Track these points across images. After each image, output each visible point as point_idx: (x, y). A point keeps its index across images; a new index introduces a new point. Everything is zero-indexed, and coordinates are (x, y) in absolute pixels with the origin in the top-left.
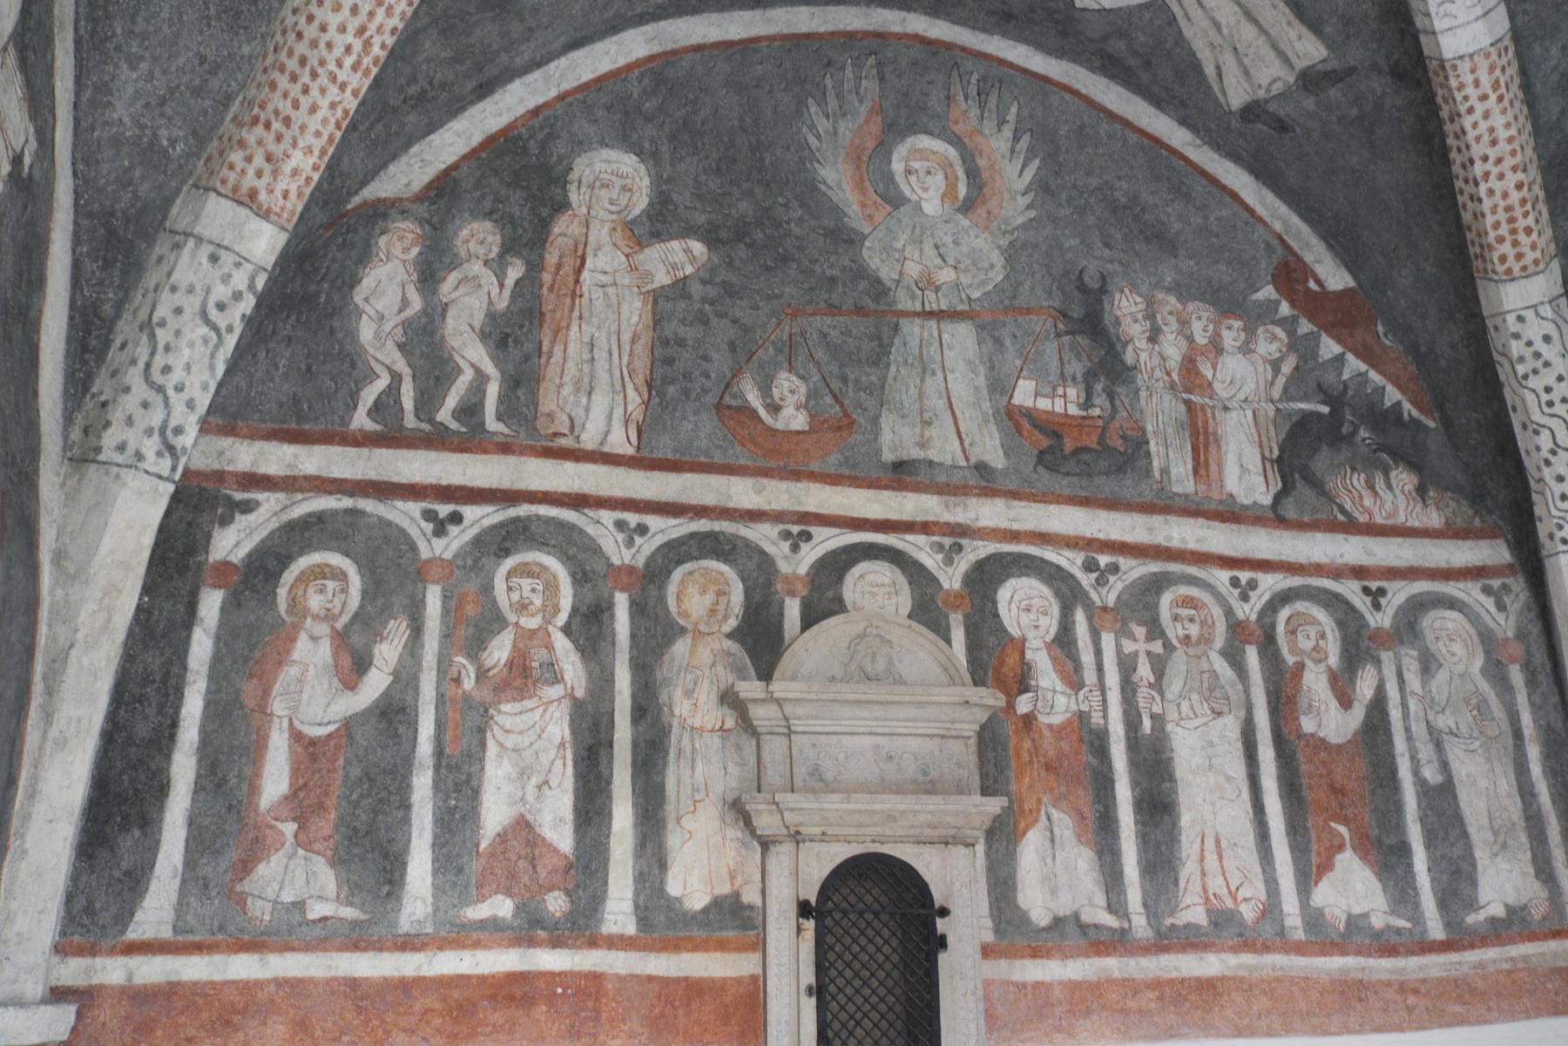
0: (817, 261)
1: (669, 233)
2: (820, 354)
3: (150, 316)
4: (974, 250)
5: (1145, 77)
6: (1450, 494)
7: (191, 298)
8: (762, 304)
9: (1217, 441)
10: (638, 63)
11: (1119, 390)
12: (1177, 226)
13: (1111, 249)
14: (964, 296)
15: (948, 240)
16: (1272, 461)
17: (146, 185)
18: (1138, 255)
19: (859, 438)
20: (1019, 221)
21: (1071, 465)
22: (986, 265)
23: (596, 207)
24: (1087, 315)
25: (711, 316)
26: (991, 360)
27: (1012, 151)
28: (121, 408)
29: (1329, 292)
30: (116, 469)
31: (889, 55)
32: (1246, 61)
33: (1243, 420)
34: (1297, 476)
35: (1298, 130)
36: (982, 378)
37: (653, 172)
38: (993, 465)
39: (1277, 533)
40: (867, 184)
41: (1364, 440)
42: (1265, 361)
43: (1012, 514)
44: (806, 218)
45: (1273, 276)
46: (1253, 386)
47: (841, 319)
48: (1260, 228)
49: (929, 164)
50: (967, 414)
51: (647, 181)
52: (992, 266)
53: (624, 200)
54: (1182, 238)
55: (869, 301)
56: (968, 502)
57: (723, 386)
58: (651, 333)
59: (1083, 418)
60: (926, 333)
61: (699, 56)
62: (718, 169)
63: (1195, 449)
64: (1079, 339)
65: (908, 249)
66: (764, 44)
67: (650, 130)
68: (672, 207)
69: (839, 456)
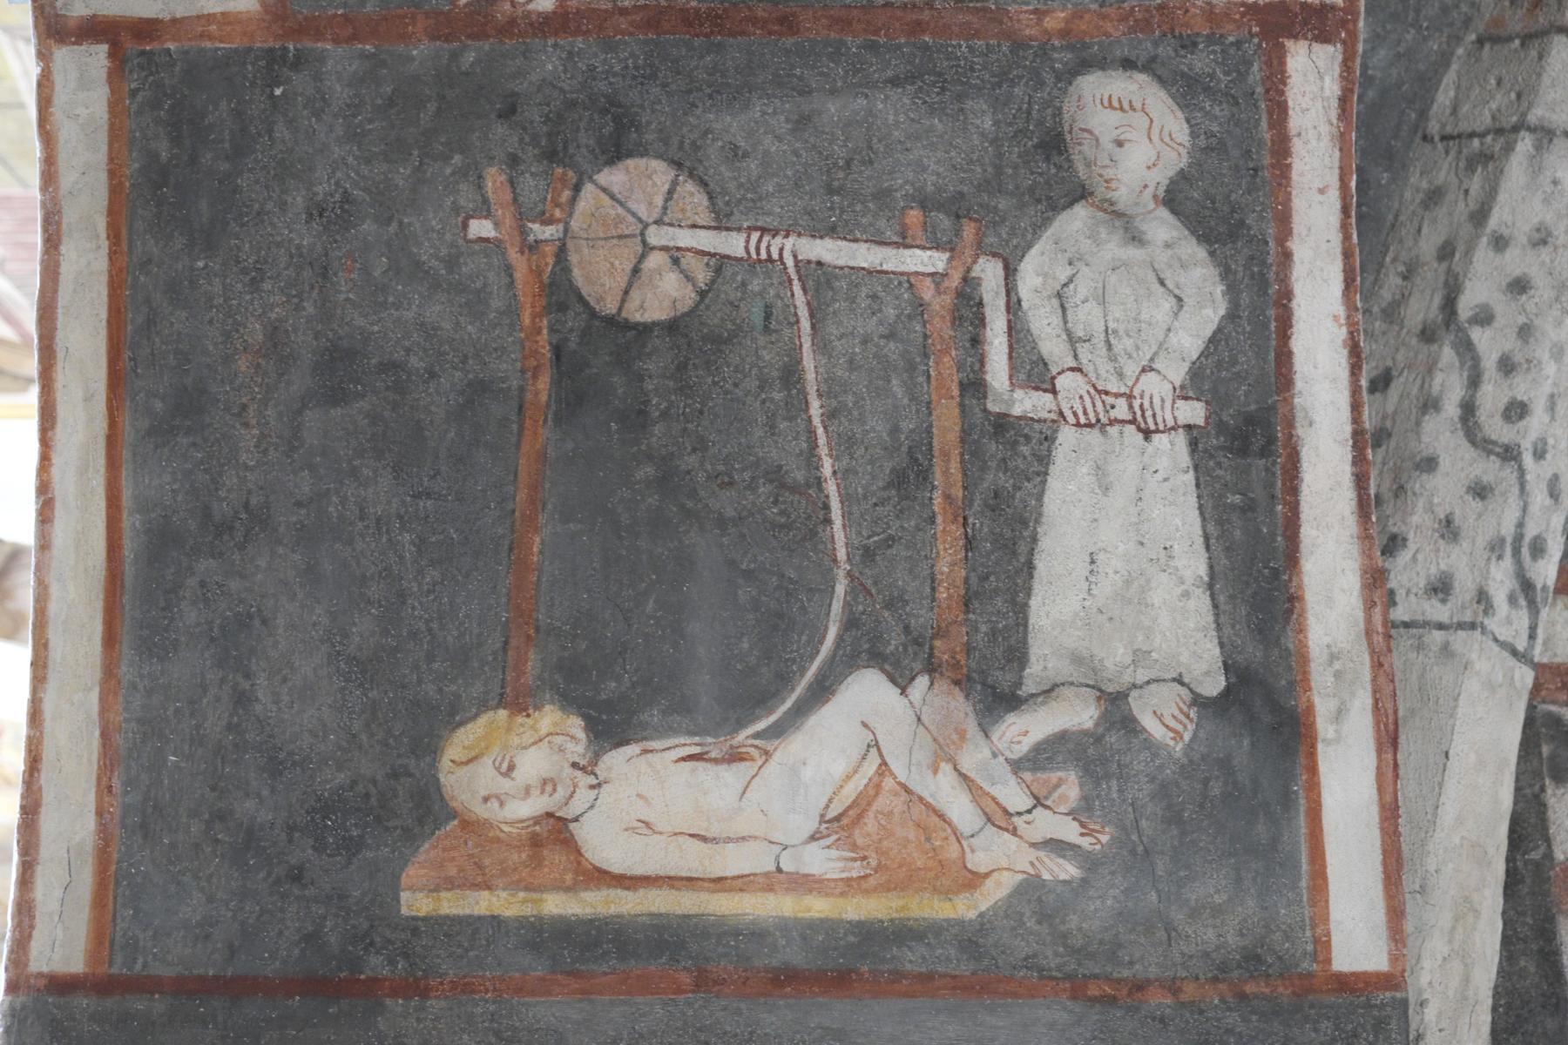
3: (1449, 305)
7: (1545, 253)
17: (1382, 53)
28: (1421, 503)
30: (1438, 636)
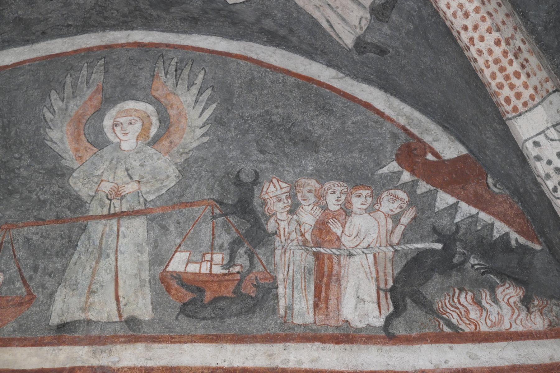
4: (155, 168)
5: (294, 40)
6: (554, 301)
9: (338, 280)
13: (264, 154)
14: (142, 200)
15: (137, 164)
16: (386, 291)
20: (195, 145)
21: (209, 312)
24: (240, 201)
26: (156, 242)
27: (196, 101)
29: (444, 161)
31: (114, 57)
32: (339, 11)
33: (364, 262)
34: (408, 301)
35: (391, 50)
38: (142, 318)
39: (387, 348)
40: (83, 137)
41: (473, 266)
42: (387, 216)
43: (150, 354)
44: (34, 164)
45: (397, 155)
46: (375, 236)
47: (44, 227)
48: (388, 125)
49: (131, 118)
50: (128, 283)
52: (168, 177)
54: (322, 140)
55: (68, 213)
56: (113, 349)
59: (225, 274)
60: (107, 229)
63: (318, 289)
64: (231, 219)
65: (105, 174)
66: (27, 64)
69: (15, 324)
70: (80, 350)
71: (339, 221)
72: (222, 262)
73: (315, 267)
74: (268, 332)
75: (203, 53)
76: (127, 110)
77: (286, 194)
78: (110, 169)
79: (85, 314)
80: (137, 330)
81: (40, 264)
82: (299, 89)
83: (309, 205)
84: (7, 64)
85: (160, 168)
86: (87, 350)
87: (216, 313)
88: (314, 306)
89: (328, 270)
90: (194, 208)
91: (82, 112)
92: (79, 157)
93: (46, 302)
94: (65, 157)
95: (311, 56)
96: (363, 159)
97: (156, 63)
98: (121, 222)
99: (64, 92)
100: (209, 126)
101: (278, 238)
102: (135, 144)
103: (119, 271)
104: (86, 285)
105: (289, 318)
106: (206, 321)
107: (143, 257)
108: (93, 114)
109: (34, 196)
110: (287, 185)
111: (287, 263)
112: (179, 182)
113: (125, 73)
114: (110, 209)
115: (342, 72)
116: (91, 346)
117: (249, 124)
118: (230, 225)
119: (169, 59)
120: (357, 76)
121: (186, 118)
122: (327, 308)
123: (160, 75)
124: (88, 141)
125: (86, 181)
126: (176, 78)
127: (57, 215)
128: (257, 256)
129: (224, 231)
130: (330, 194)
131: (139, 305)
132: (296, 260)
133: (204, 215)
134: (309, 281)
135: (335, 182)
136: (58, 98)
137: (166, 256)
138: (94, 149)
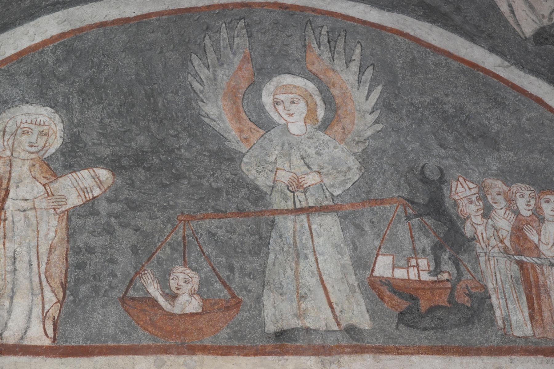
0: (204, 177)
1: (80, 165)
2: (209, 249)
4: (333, 158)
5: (458, 19)
8: (159, 214)
10: (52, 40)
11: (462, 257)
12: (496, 127)
13: (445, 149)
14: (327, 194)
15: (312, 151)
18: (466, 151)
19: (245, 314)
20: (369, 133)
22: (344, 169)
23: (18, 149)
24: (431, 200)
25: (117, 227)
26: (353, 243)
27: (359, 81)
31: (255, 18)
36: (347, 257)
37: (65, 119)
38: (361, 327)
40: (243, 115)
44: (194, 144)
47: (226, 220)
49: (293, 96)
50: (336, 288)
51: (60, 126)
52: (349, 169)
53: (41, 142)
54: (501, 136)
55: (249, 205)
56: (342, 360)
57: (127, 282)
58: (65, 245)
59: (434, 282)
60: (298, 226)
61: (102, 30)
62: (120, 112)
64: (426, 220)
65: (279, 161)
66: (154, 18)
67: (62, 88)
68: (82, 145)
70: (307, 361)
71: (534, 228)
72: (429, 268)
73: (521, 277)
74: (491, 344)
75: (355, 24)
76: (285, 86)
77: (475, 196)
78: (284, 156)
79: (301, 321)
80: (361, 340)
81: (235, 263)
82: (465, 75)
83: (501, 209)
84: (129, 16)
85: (339, 158)
86: (314, 360)
87: (436, 323)
88: (530, 318)
89: (534, 280)
90: (385, 206)
91: (234, 84)
92: (246, 139)
93: (255, 307)
94: (228, 138)
95: (472, 38)
96: (545, 161)
97: (305, 31)
98: (311, 219)
99: (207, 57)
100: (379, 111)
101: (478, 244)
102: (304, 128)
103: (323, 274)
104: (293, 289)
105: (508, 330)
106: (427, 332)
107: (345, 259)
108: (249, 87)
109: (204, 182)
110: (475, 186)
111: (493, 271)
112: (362, 175)
113: (272, 39)
114: (294, 202)
115: (506, 60)
116: (317, 357)
117: (421, 112)
118: (427, 227)
119: (319, 27)
120: (524, 66)
121: (352, 100)
122: (543, 320)
123: (312, 45)
124: (250, 119)
125: (259, 168)
126: (331, 51)
127: (237, 206)
128: (463, 263)
129: (422, 234)
130: (519, 198)
131: (355, 313)
132: (502, 269)
133: (398, 215)
134: (519, 292)
135: (521, 185)
136: (202, 65)
137: (369, 259)
138: (260, 130)
